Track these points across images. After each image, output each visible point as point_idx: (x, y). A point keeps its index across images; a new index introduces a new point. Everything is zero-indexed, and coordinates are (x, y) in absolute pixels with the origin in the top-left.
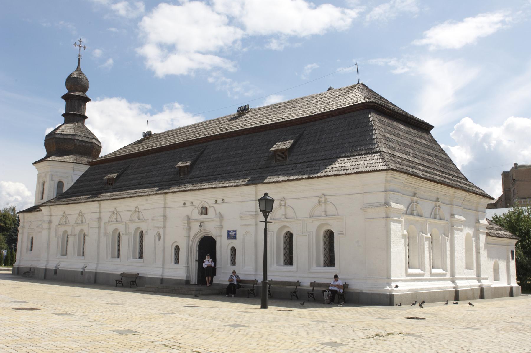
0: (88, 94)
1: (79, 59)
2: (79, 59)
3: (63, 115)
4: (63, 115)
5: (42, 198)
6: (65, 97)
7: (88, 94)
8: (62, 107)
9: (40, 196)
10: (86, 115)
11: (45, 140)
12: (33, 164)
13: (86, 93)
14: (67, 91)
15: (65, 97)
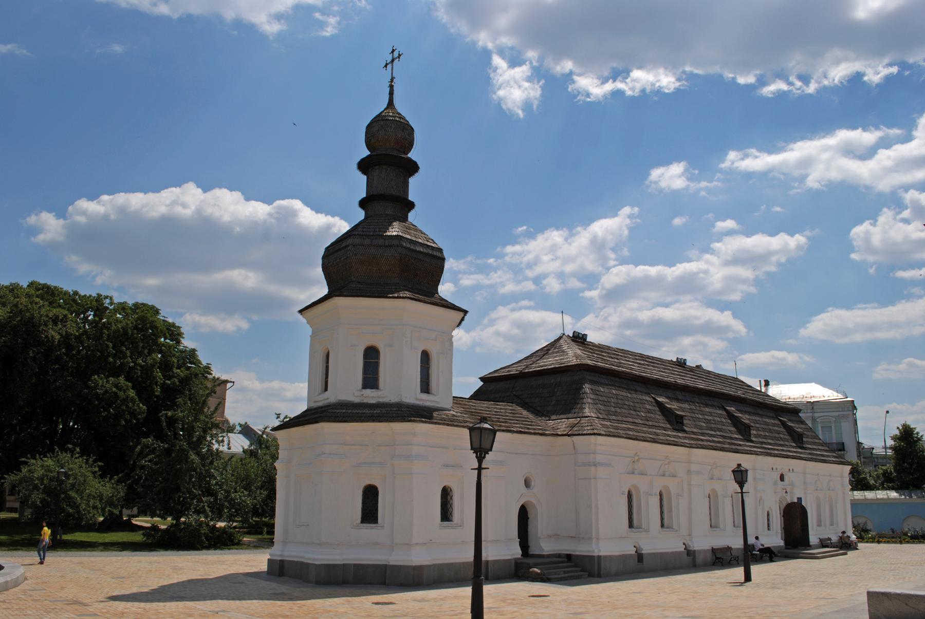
0: (412, 155)
1: (391, 87)
2: (391, 87)
3: (363, 204)
4: (363, 204)
5: (326, 389)
6: (364, 166)
7: (412, 155)
8: (359, 185)
9: (319, 385)
10: (411, 198)
11: (324, 258)
12: (301, 311)
13: (409, 155)
14: (366, 153)
15: (364, 166)
